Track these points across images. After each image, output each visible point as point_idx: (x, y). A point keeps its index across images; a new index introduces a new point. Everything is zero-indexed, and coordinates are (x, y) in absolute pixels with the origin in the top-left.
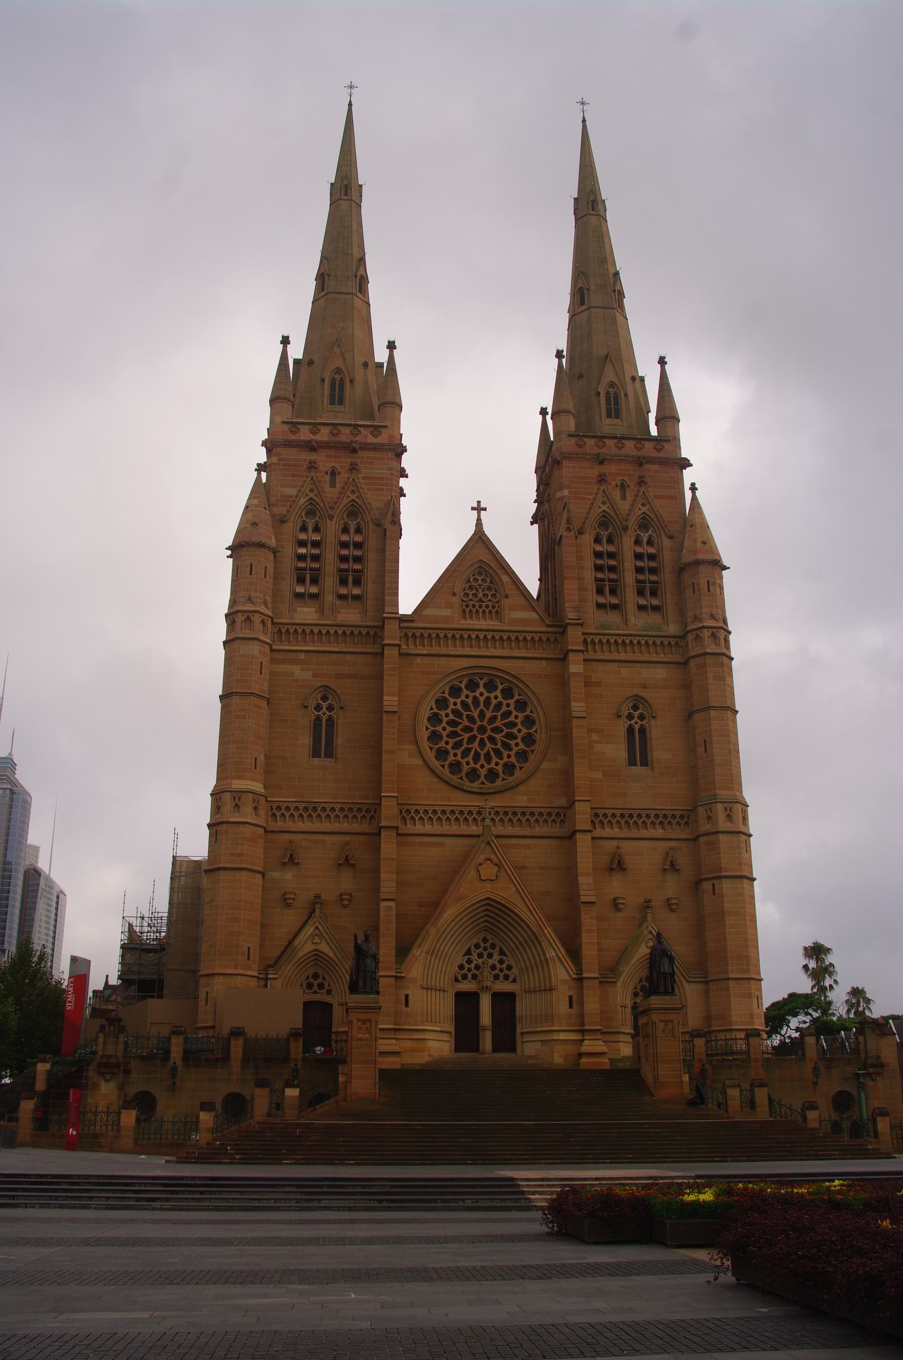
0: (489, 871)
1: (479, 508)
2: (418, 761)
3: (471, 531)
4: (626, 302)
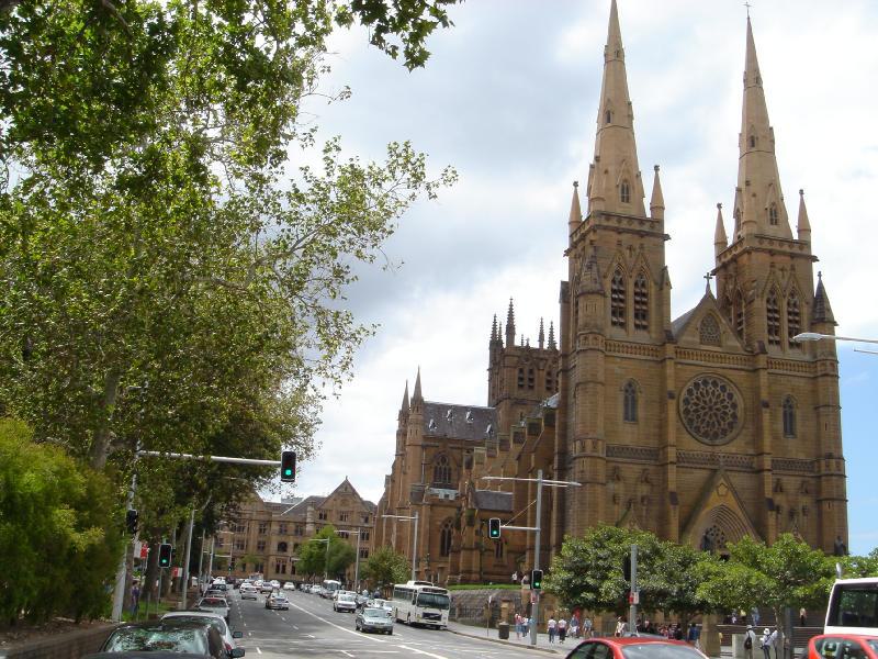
0: (722, 490)
3: (703, 293)
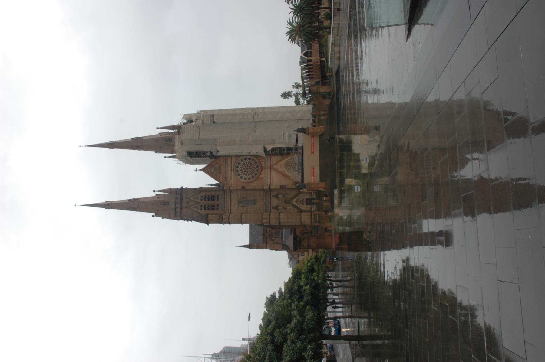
1: (196, 170)
2: (255, 182)
3: (202, 172)
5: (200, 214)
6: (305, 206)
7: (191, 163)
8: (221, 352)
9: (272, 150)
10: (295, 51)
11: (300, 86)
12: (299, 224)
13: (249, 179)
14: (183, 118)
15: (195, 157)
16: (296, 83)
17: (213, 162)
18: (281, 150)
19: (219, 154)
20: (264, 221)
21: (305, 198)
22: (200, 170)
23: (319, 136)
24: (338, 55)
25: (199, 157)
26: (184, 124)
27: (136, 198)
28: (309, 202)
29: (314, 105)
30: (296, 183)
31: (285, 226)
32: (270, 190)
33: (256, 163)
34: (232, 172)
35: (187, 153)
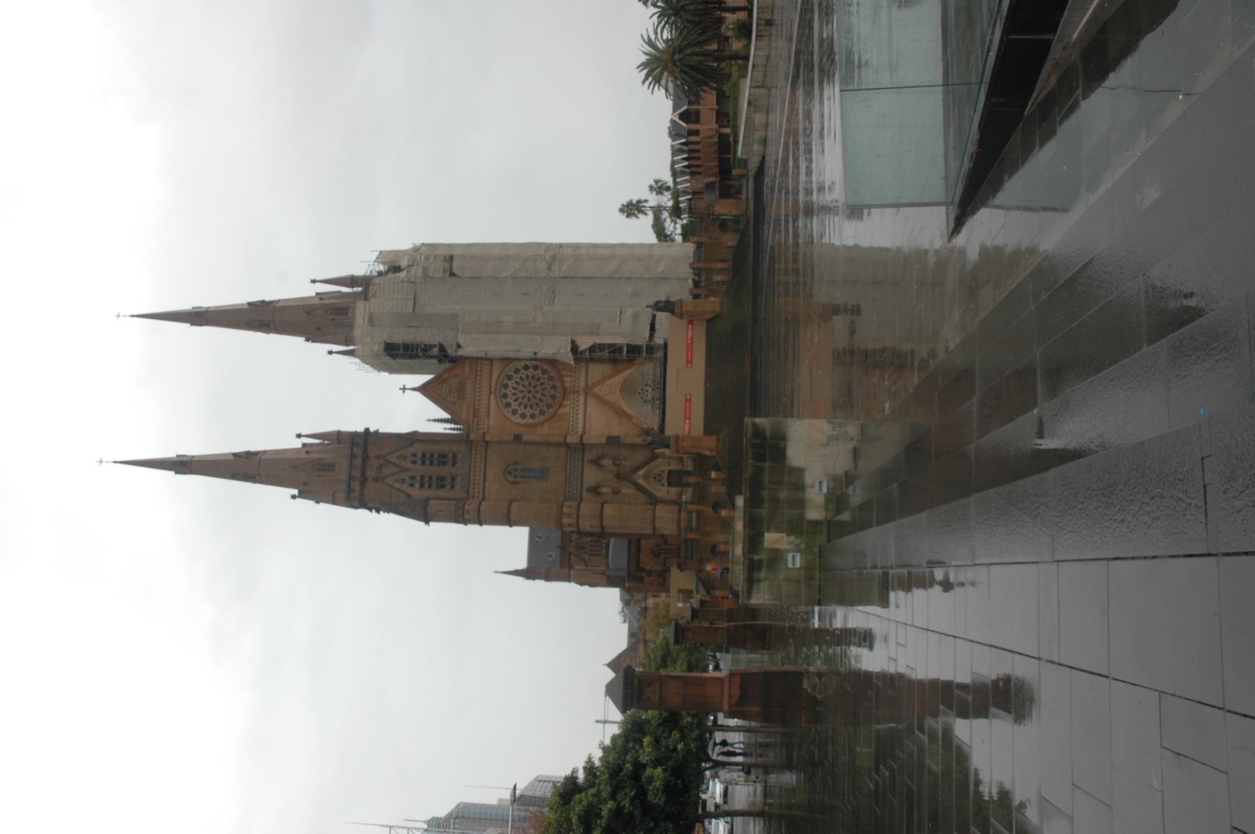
1: (404, 389)
2: (546, 426)
3: (418, 395)
4: (267, 299)
5: (409, 496)
6: (666, 488)
7: (392, 371)
8: (449, 816)
9: (592, 349)
10: (659, 108)
11: (668, 189)
12: (649, 531)
13: (533, 416)
14: (377, 260)
15: (403, 357)
16: (657, 182)
17: (448, 372)
18: (614, 351)
19: (460, 353)
20: (565, 521)
21: (667, 469)
22: (414, 389)
23: (708, 321)
24: (763, 133)
25: (411, 357)
26: (380, 274)
27: (253, 449)
28: (675, 478)
29: (699, 246)
30: (647, 432)
31: (616, 535)
32: (583, 446)
33: (551, 378)
34: (493, 396)
35: (382, 347)
